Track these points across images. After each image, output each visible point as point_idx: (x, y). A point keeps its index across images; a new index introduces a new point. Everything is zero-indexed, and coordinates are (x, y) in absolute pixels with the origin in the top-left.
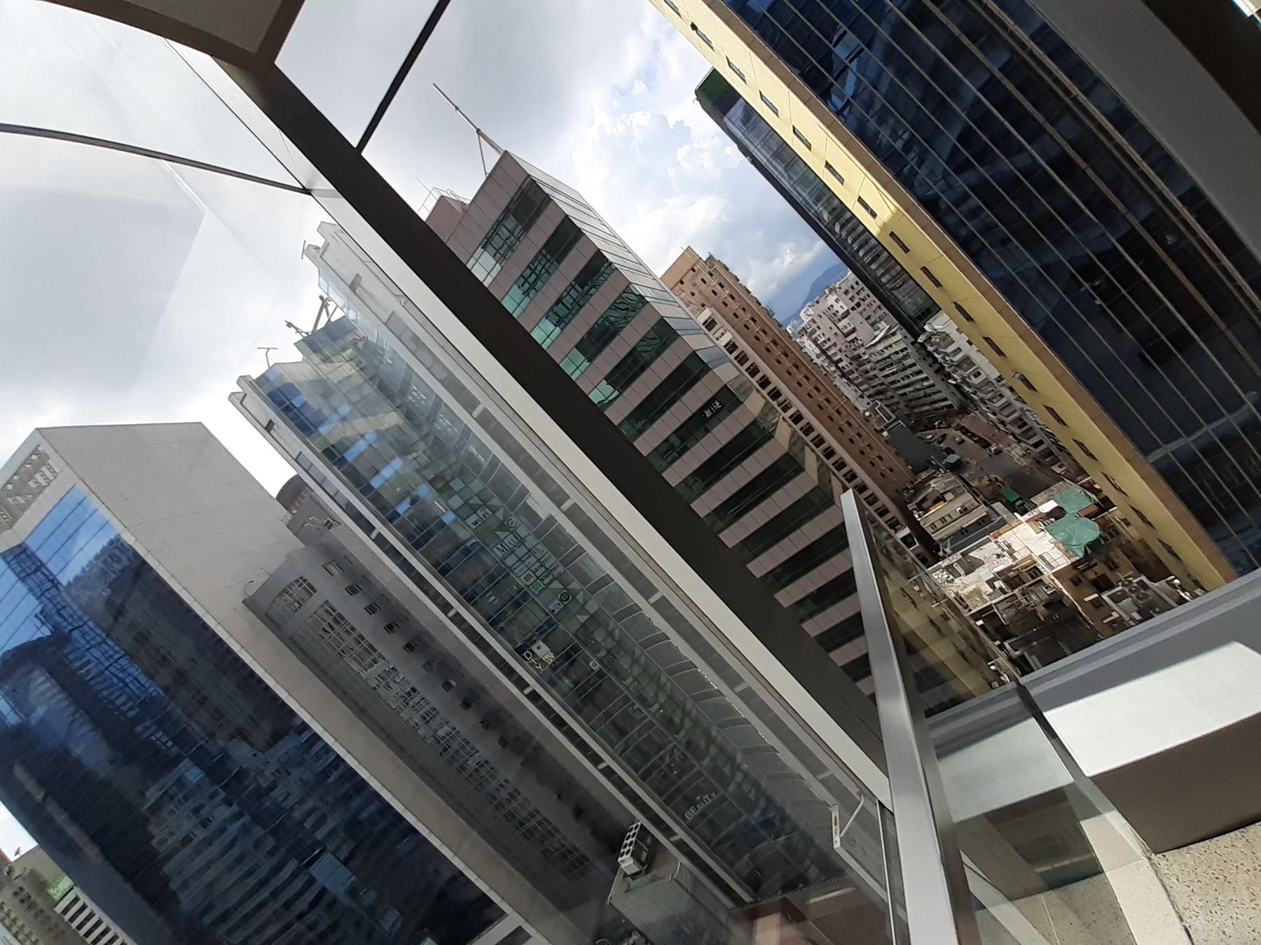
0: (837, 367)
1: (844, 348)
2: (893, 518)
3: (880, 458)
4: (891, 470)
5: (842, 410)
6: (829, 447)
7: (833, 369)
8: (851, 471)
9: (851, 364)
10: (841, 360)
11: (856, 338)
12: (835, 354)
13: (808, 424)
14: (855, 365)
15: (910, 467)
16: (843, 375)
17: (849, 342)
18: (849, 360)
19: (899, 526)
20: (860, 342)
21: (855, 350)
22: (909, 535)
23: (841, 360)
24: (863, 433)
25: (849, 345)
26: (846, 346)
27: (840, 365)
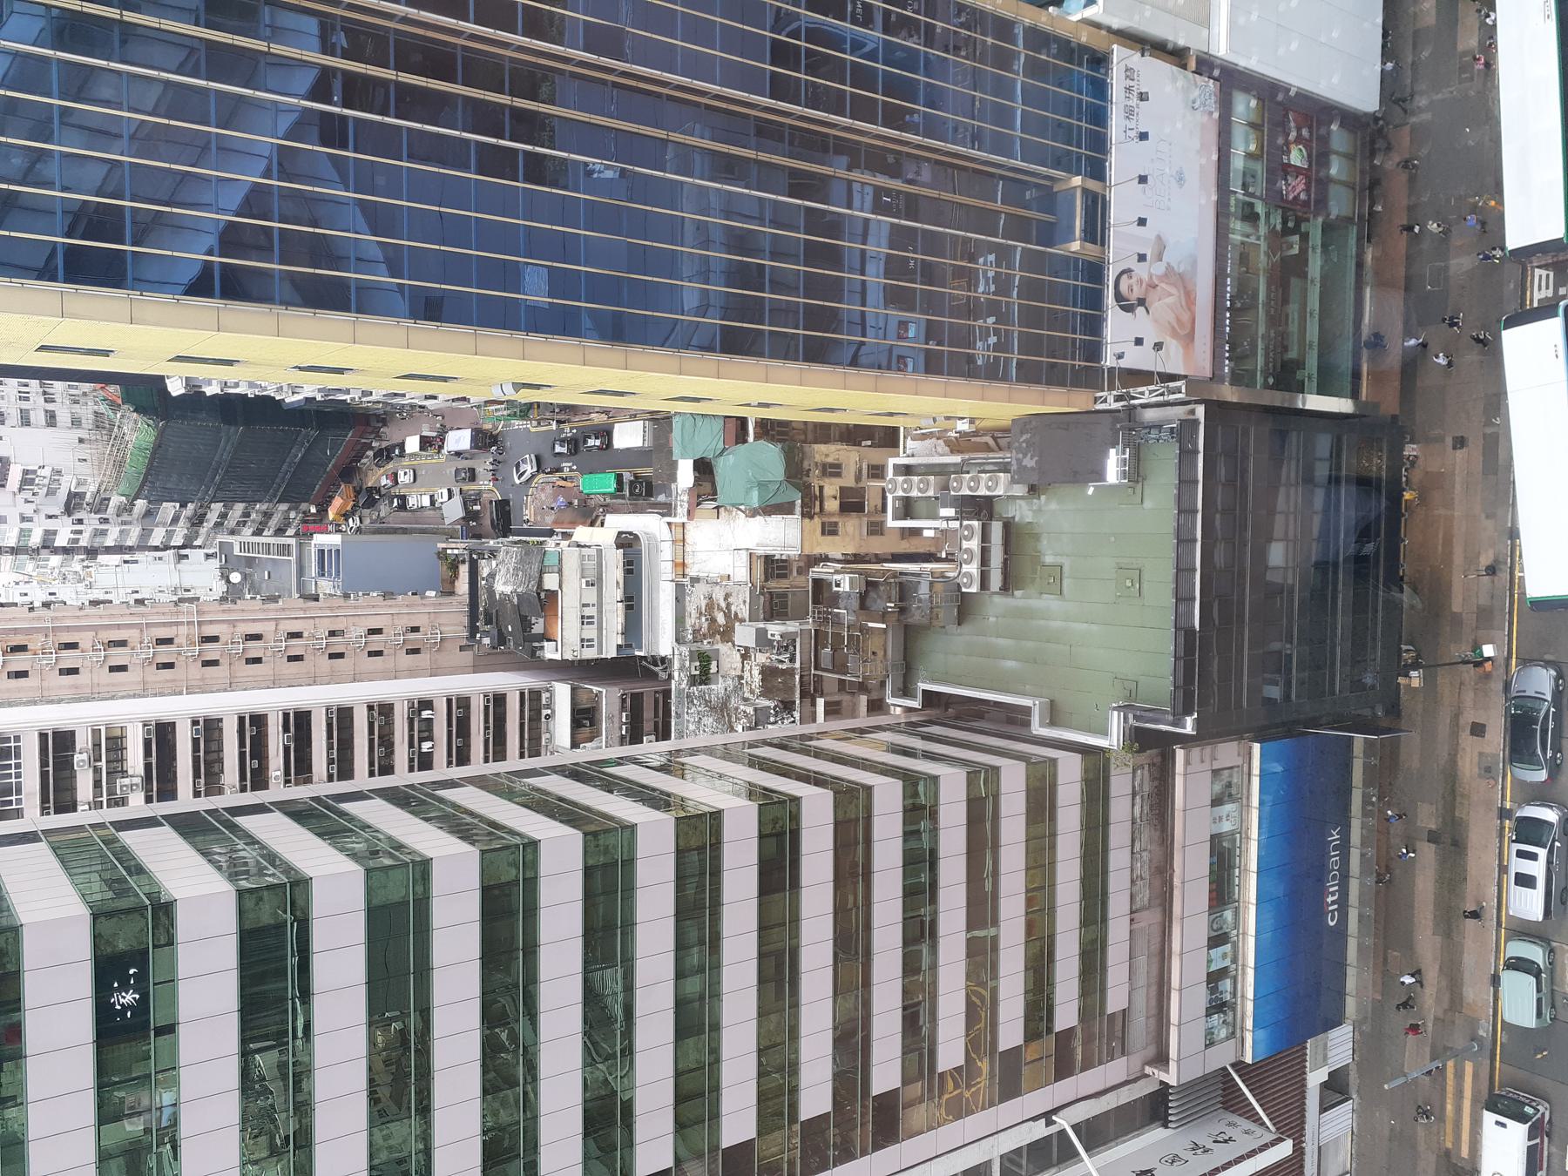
0: (56, 551)
1: (28, 510)
2: (522, 694)
3: (373, 632)
4: (415, 629)
5: (210, 631)
6: (286, 716)
7: (55, 560)
8: (370, 708)
9: (80, 522)
10: (49, 535)
11: (26, 472)
12: (24, 534)
13: (195, 723)
14: (91, 522)
15: (433, 593)
16: (92, 553)
17: (21, 489)
18: (68, 520)
19: (544, 696)
20: (46, 472)
21: (51, 493)
22: (574, 690)
23: (49, 535)
24: (295, 627)
25: (27, 495)
26: (27, 501)
27: (61, 541)
